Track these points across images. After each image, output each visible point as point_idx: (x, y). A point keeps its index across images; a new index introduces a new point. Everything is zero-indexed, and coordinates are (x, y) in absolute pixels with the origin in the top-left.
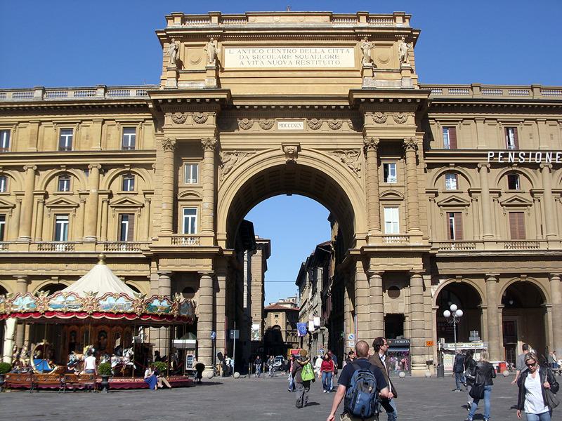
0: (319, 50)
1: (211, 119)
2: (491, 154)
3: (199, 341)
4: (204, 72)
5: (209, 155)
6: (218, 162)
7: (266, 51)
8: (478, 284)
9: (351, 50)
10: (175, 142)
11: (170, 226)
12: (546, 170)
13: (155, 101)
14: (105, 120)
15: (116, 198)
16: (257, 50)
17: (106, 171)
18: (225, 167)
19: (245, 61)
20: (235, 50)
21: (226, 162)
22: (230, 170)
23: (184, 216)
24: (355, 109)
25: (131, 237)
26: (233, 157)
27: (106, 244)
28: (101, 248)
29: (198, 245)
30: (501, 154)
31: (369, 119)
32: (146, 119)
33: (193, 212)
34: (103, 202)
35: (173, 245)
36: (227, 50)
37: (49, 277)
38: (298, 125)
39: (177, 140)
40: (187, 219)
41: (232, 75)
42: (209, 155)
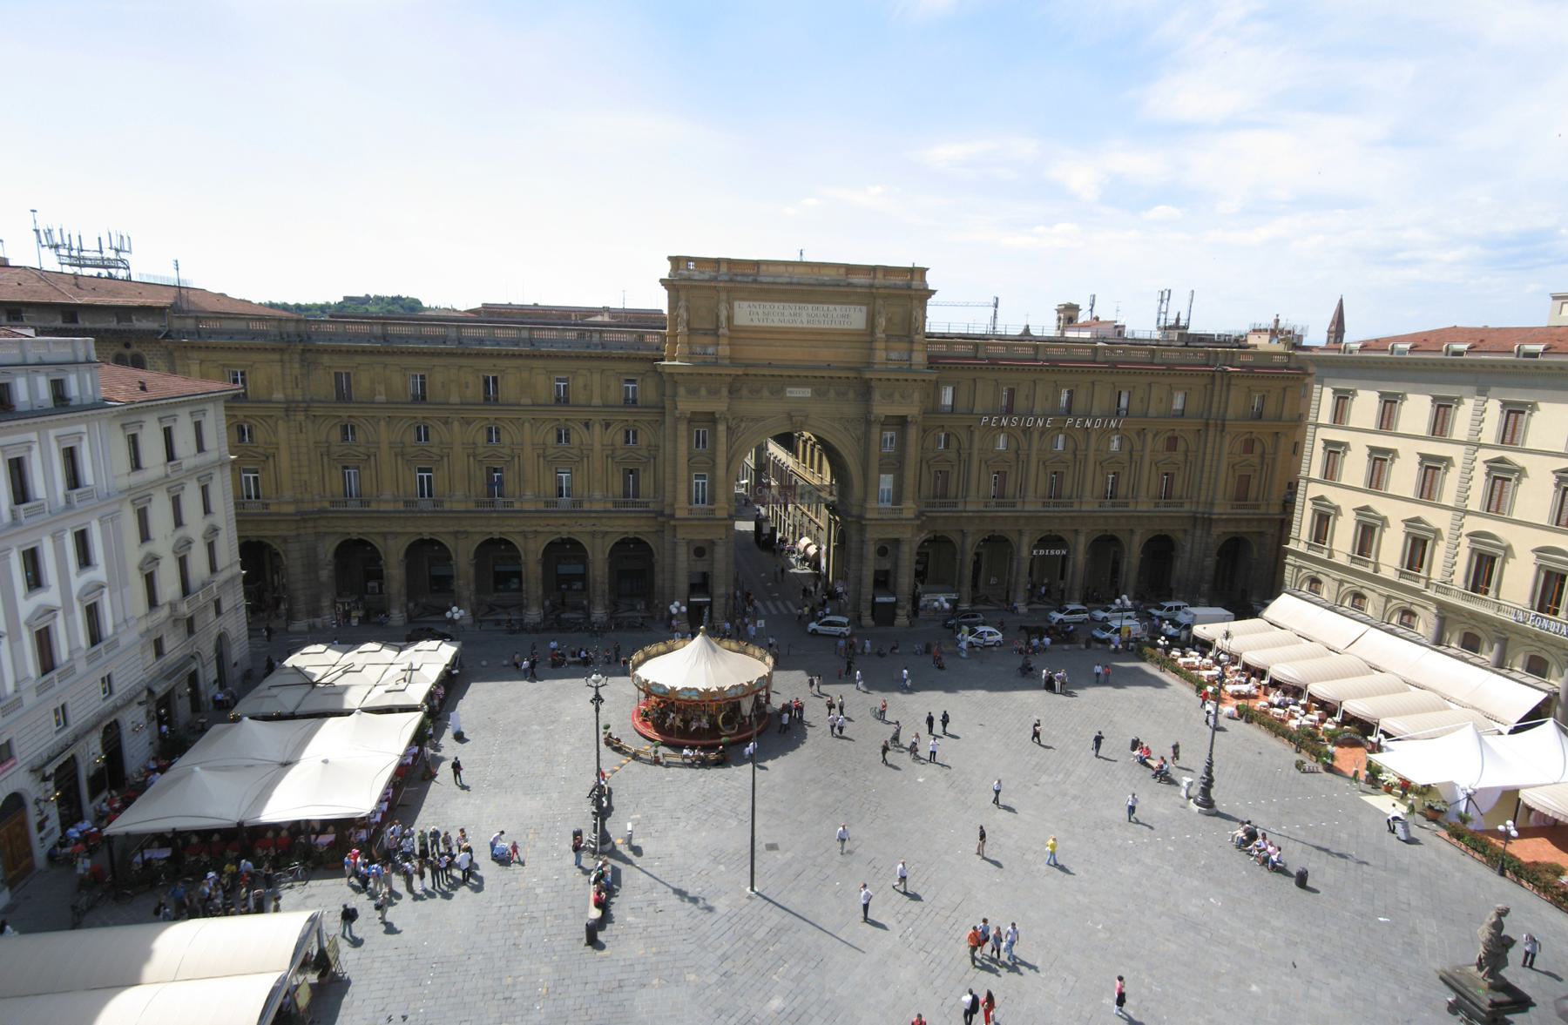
0: (831, 307)
1: (725, 392)
7: (778, 307)
8: (956, 538)
9: (864, 309)
12: (1036, 435)
15: (619, 452)
16: (768, 304)
19: (755, 318)
20: (745, 304)
24: (860, 384)
25: (636, 495)
27: (615, 504)
28: (610, 506)
31: (877, 396)
33: (704, 477)
36: (736, 304)
38: (806, 392)
42: (722, 428)
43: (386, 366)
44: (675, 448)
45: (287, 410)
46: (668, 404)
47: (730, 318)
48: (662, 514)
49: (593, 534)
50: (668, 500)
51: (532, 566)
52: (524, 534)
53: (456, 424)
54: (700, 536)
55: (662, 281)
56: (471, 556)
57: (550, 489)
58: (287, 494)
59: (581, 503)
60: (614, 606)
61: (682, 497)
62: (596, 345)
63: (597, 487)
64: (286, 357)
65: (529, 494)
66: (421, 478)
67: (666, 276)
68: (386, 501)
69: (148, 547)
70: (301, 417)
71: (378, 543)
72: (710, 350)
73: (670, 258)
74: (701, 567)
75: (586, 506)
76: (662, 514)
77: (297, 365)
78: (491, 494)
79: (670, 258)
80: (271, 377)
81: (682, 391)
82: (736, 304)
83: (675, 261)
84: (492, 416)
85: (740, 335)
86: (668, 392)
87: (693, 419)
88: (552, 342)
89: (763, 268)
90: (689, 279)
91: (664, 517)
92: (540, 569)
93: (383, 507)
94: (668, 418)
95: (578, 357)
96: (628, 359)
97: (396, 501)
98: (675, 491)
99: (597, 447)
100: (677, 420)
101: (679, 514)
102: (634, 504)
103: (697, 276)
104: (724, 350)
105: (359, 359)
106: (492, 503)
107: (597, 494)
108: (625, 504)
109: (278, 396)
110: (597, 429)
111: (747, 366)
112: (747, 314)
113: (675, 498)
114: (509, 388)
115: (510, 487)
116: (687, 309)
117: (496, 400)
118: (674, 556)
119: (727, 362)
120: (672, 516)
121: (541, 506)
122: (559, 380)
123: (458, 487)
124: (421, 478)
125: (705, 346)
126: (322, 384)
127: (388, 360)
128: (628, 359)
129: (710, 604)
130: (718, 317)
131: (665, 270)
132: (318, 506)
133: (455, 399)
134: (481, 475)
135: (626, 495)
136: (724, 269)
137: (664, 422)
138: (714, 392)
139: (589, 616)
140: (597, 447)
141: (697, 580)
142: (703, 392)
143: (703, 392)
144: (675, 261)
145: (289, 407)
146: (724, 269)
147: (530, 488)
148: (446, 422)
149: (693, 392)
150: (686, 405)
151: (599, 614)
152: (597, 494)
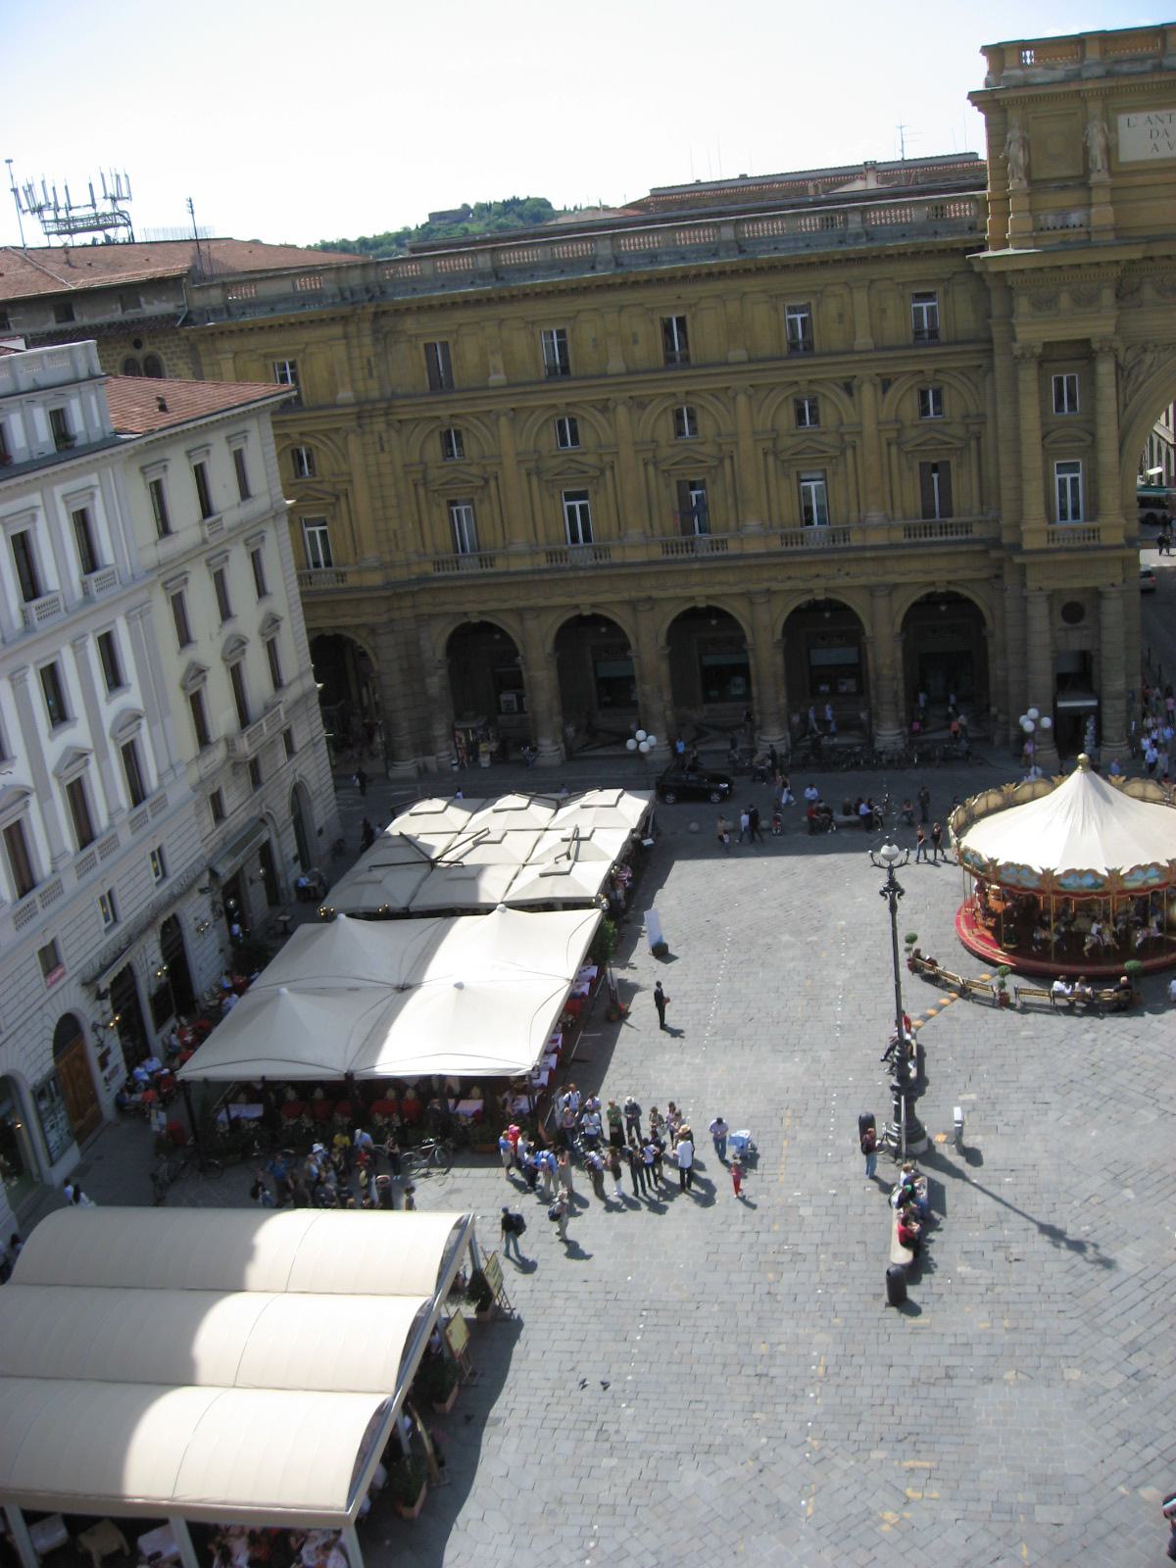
1: (1107, 296)
3: (1107, 702)
10: (1038, 350)
11: (1042, 509)
14: (872, 281)
18: (1133, 377)
20: (1139, 119)
21: (1132, 368)
22: (1141, 384)
23: (1057, 477)
25: (947, 512)
26: (1148, 358)
27: (909, 531)
28: (899, 536)
29: (1096, 542)
32: (955, 273)
33: (1073, 468)
34: (889, 444)
35: (1051, 545)
36: (1122, 120)
37: (810, 591)
39: (1045, 344)
40: (1063, 483)
41: (1139, 180)
42: (1105, 369)
43: (501, 322)
44: (1016, 414)
45: (359, 416)
46: (998, 332)
47: (1110, 151)
48: (996, 543)
49: (871, 590)
50: (1007, 517)
51: (766, 655)
52: (748, 596)
53: (621, 410)
54: (1074, 582)
55: (974, 97)
56: (662, 640)
57: (791, 511)
58: (371, 556)
59: (846, 534)
60: (914, 720)
61: (1034, 509)
62: (858, 236)
63: (876, 504)
64: (352, 329)
65: (752, 523)
66: (571, 510)
67: (980, 86)
68: (519, 555)
69: (230, 628)
70: (379, 425)
71: (510, 625)
72: (1075, 218)
73: (986, 50)
74: (1077, 641)
75: (856, 539)
76: (996, 543)
77: (367, 341)
78: (687, 529)
79: (986, 50)
80: (333, 364)
81: (1023, 305)
82: (1122, 120)
83: (996, 53)
84: (680, 389)
85: (1128, 180)
86: (996, 311)
87: (1049, 356)
88: (774, 241)
90: (1027, 85)
91: (1000, 552)
92: (779, 659)
93: (517, 565)
94: (997, 360)
95: (824, 263)
96: (917, 255)
97: (534, 553)
98: (1019, 498)
99: (870, 427)
100: (1017, 361)
101: (1031, 542)
102: (944, 529)
103: (1041, 76)
104: (1103, 215)
105: (460, 316)
106: (691, 546)
107: (875, 516)
108: (928, 530)
109: (345, 395)
110: (867, 394)
111: (1150, 240)
112: (1146, 136)
113: (1020, 512)
114: (707, 337)
115: (718, 515)
116: (1026, 145)
117: (686, 359)
118: (1024, 622)
119: (1110, 237)
120: (1017, 548)
121: (776, 544)
122: (793, 310)
123: (634, 527)
124: (571, 510)
125: (1064, 212)
126: (407, 367)
127: (503, 311)
128: (917, 255)
129: (1097, 712)
130: (1086, 151)
131: (977, 74)
132: (416, 570)
133: (616, 365)
134: (667, 497)
135: (928, 512)
136: (1093, 53)
137: (991, 369)
138: (1086, 300)
139: (870, 740)
140: (870, 427)
141: (1070, 667)
142: (1065, 301)
143: (1065, 301)
144: (996, 53)
145: (363, 411)
146: (1093, 53)
147: (753, 519)
148: (604, 408)
149: (1044, 304)
150: (1033, 331)
151: (889, 736)
152: (875, 516)
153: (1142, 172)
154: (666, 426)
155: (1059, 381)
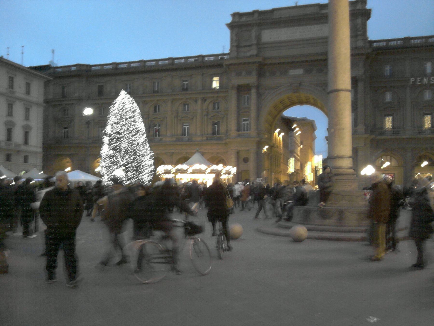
1: (254, 73)
2: (413, 80)
4: (249, 46)
5: (253, 91)
6: (259, 95)
13: (226, 65)
17: (205, 100)
30: (419, 79)
33: (247, 120)
42: (253, 91)
47: (259, 37)
57: (179, 132)
89: (275, 12)
109: (77, 94)
110: (199, 102)
112: (269, 36)
116: (236, 35)
136: (256, 15)
142: (244, 73)
143: (244, 73)
146: (256, 15)
149: (239, 74)
153: (268, 44)
154: (152, 109)
155: (244, 97)
